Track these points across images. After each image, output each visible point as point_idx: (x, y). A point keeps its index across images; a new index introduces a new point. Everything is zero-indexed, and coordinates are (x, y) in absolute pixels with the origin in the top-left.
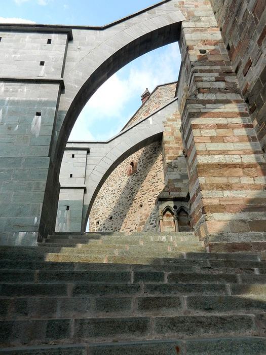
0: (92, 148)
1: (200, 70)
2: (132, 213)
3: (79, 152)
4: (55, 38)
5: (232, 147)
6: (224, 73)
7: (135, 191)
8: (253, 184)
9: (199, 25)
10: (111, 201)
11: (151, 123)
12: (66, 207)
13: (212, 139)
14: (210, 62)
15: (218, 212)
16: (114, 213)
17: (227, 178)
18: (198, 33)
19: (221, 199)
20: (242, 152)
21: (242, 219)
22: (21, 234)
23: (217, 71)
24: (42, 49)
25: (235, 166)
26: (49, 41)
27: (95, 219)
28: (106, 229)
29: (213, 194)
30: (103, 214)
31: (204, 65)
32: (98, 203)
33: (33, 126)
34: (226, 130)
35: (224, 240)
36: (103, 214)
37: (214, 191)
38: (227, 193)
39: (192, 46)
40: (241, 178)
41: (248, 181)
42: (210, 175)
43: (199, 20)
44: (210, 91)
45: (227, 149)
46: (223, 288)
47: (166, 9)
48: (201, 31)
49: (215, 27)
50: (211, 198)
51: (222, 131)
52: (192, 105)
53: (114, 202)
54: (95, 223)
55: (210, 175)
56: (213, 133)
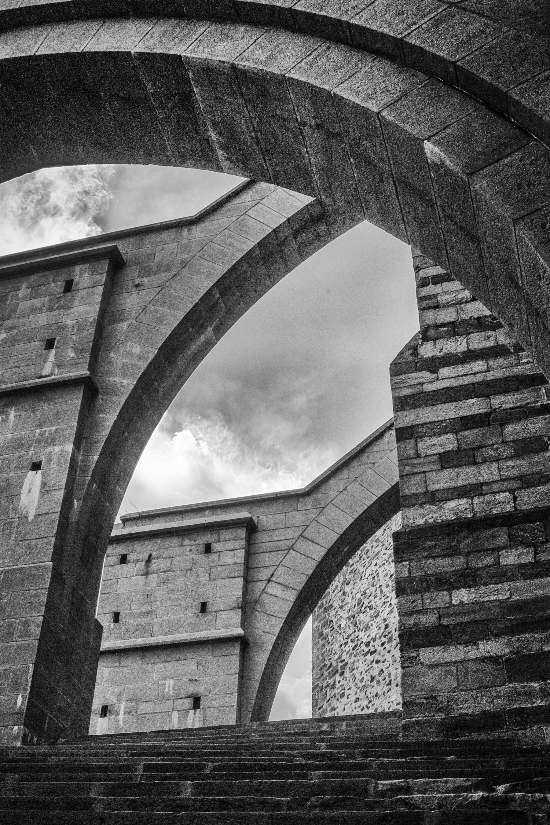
0: (265, 518)
1: (434, 277)
3: (226, 534)
5: (495, 472)
8: (530, 563)
10: (367, 678)
12: (191, 700)
13: (446, 460)
15: (431, 644)
17: (466, 557)
19: (442, 612)
21: (492, 654)
25: (489, 522)
32: (336, 691)
33: (23, 497)
34: (483, 430)
35: (438, 711)
37: (427, 595)
38: (462, 596)
41: (519, 556)
44: (455, 329)
45: (481, 479)
50: (418, 612)
51: (471, 435)
52: (403, 377)
53: (373, 678)
56: (448, 442)
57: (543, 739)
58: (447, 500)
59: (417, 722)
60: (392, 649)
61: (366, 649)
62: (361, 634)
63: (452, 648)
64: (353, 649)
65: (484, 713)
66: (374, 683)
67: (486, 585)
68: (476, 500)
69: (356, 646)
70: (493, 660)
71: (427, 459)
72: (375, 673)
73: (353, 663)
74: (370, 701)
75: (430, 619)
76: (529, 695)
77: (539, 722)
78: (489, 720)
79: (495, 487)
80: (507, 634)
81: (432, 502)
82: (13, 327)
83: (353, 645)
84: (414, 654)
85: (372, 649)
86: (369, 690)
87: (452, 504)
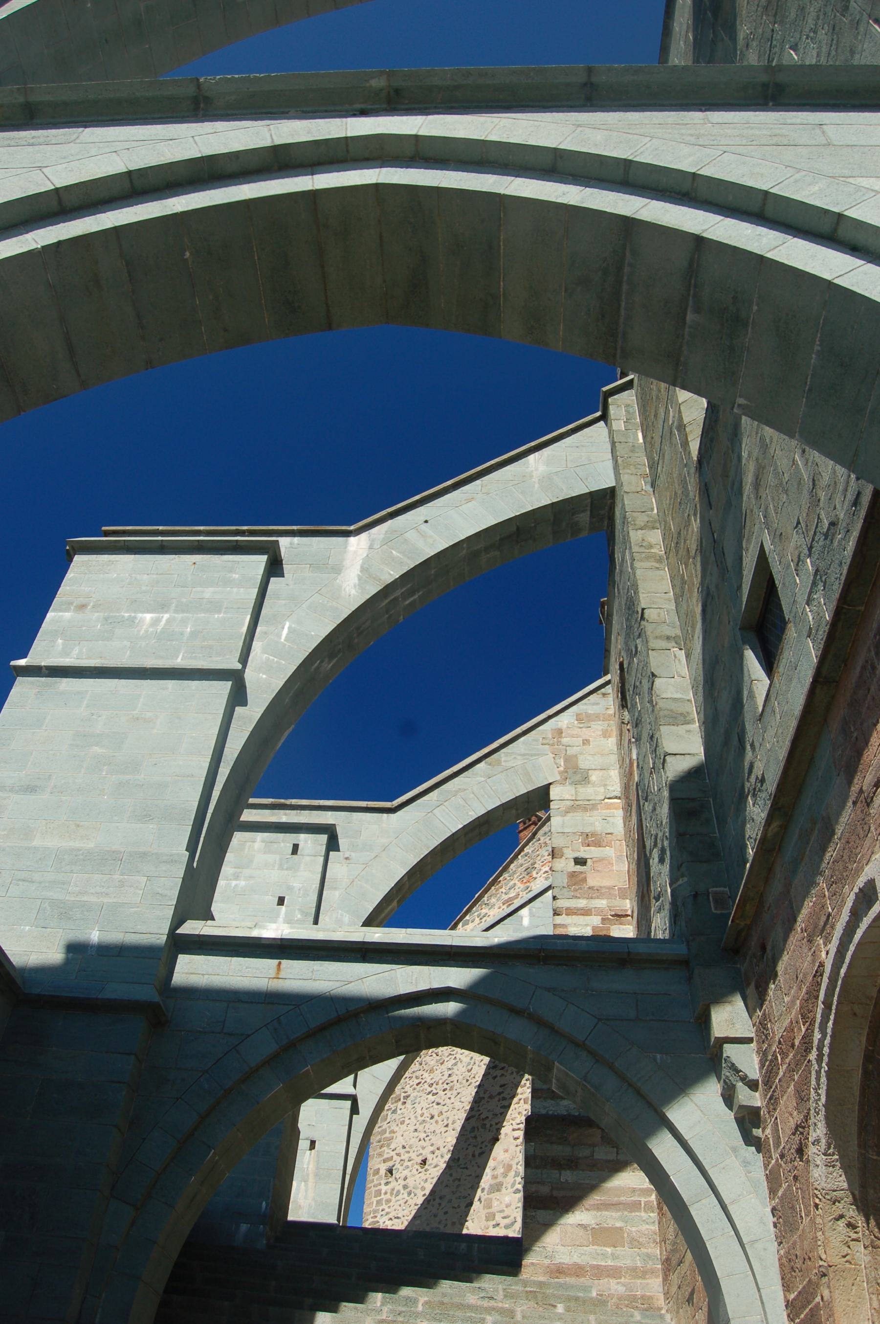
2: (473, 1156)
4: (306, 842)
6: (612, 916)
8: (613, 1161)
9: (587, 792)
11: (526, 922)
12: (309, 1142)
14: (589, 888)
16: (432, 1149)
18: (578, 816)
21: (583, 1222)
22: (244, 1227)
23: (599, 911)
24: (283, 869)
26: (295, 849)
27: (385, 1161)
30: (404, 1147)
31: (576, 897)
32: (395, 1116)
36: (404, 1147)
40: (596, 1149)
43: (585, 779)
47: (523, 751)
48: (585, 809)
49: (616, 798)
50: (538, 1183)
53: (432, 1117)
54: (383, 1172)
57: (610, 1289)
59: (533, 1264)
60: (453, 1097)
61: (429, 1089)
62: (426, 1075)
64: (417, 1085)
66: (433, 1121)
67: (583, 1170)
69: (419, 1083)
70: (584, 1227)
72: (436, 1113)
73: (416, 1098)
74: (427, 1136)
75: (545, 1190)
76: (604, 1256)
77: (608, 1276)
78: (578, 1270)
80: (595, 1209)
82: (251, 877)
83: (418, 1081)
85: (435, 1091)
86: (427, 1126)
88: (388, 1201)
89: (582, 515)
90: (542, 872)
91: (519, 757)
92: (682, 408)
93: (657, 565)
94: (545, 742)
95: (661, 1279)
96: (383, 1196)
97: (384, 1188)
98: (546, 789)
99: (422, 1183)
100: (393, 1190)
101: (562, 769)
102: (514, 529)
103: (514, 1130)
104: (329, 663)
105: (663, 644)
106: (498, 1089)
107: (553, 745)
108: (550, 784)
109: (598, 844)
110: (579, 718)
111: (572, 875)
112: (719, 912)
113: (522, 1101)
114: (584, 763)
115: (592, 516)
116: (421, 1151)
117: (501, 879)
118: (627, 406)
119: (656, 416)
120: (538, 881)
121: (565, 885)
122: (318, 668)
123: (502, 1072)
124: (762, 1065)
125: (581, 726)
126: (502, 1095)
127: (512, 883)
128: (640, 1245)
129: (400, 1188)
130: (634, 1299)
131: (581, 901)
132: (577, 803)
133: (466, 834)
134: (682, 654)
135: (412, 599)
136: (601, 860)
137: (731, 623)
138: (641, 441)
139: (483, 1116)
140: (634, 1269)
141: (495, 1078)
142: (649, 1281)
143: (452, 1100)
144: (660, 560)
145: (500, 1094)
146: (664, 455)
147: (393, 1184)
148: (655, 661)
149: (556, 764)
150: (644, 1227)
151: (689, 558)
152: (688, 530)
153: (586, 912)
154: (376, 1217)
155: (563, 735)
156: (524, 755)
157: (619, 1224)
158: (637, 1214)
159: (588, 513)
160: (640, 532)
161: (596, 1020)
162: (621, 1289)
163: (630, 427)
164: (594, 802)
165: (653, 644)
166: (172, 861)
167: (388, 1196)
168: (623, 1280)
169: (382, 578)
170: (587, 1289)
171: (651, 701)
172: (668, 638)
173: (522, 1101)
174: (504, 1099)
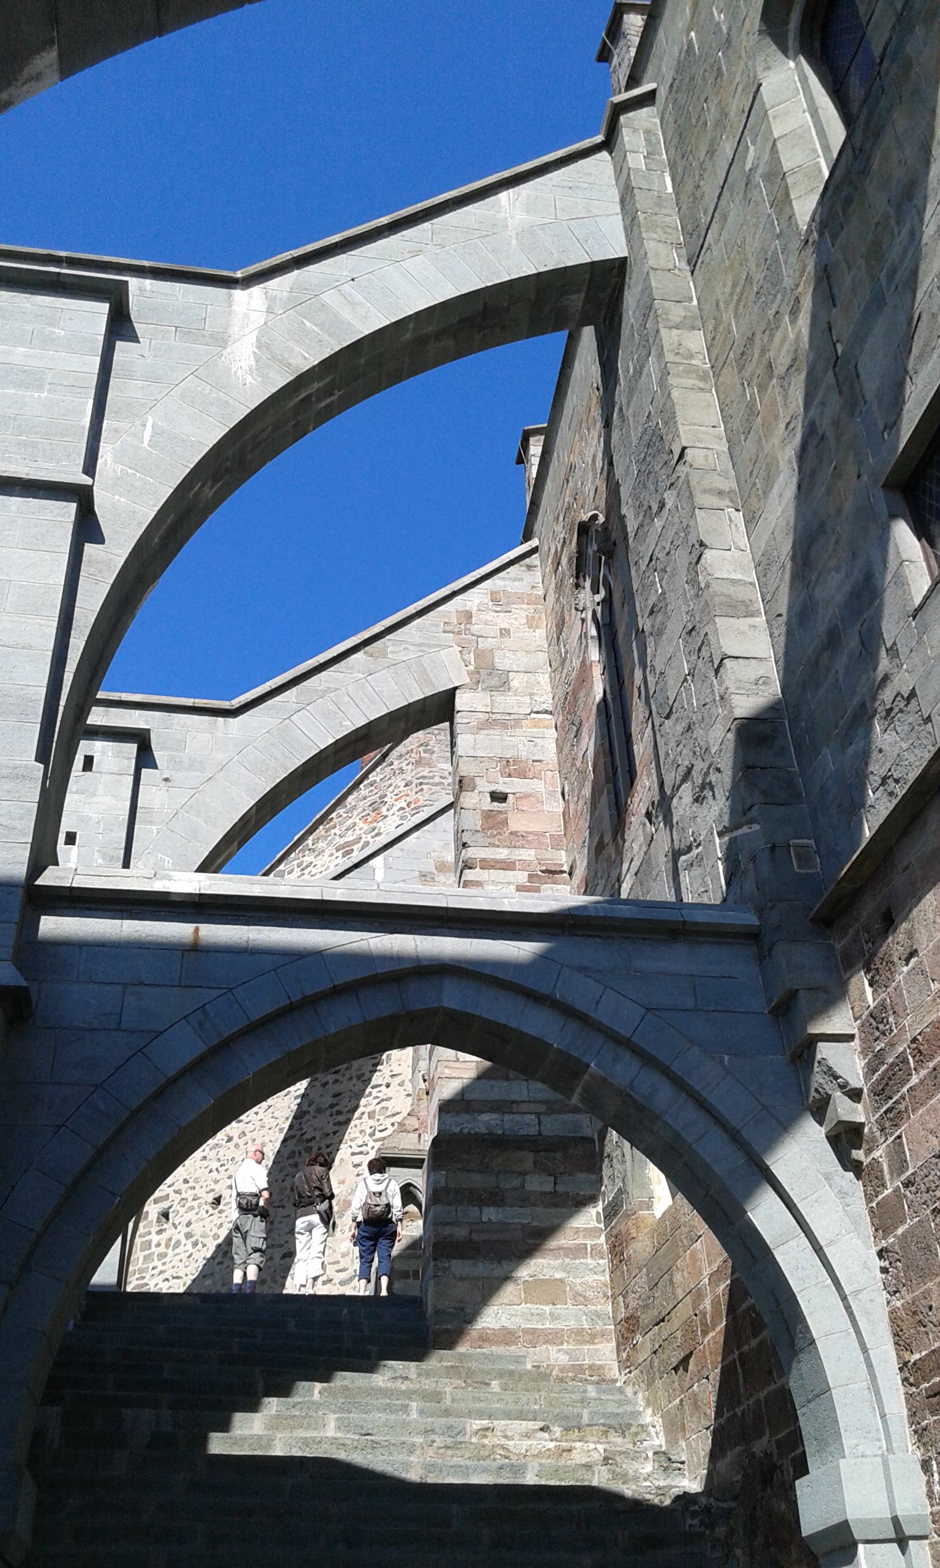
1: (483, 860)
4: (104, 753)
5: (525, 1092)
6: (542, 872)
7: (312, 1109)
8: (550, 1193)
9: (506, 702)
11: (379, 876)
14: (511, 833)
17: (497, 1176)
18: (495, 734)
20: (542, 1108)
23: (525, 865)
28: (195, 1244)
29: (460, 1215)
30: (186, 1181)
31: (494, 845)
36: (186, 1181)
37: (460, 1208)
38: (491, 1214)
39: (473, 779)
40: (528, 1177)
41: (541, 1184)
42: (460, 1166)
43: (504, 685)
45: (513, 1097)
46: (405, 1408)
47: (417, 640)
48: (504, 725)
49: (546, 712)
53: (230, 1139)
55: (460, 1166)
57: (549, 1359)
58: (482, 1112)
63: (480, 1264)
65: (504, 1328)
68: (507, 1117)
71: (465, 1065)
75: (461, 1233)
76: (541, 1316)
77: (546, 1342)
79: (524, 1107)
81: (467, 1112)
84: (447, 1265)
86: (222, 1151)
87: (485, 1117)
88: (163, 1256)
89: (574, 297)
90: (395, 809)
91: (411, 648)
92: (779, 145)
93: (701, 384)
94: (447, 628)
95: (614, 1344)
96: (153, 1249)
97: (155, 1238)
98: (451, 693)
99: (215, 1230)
100: (170, 1239)
101: (472, 668)
102: (481, 307)
103: (353, 1154)
104: (212, 487)
105: (715, 501)
106: (330, 1100)
107: (459, 633)
108: (456, 688)
109: (522, 775)
110: (495, 598)
111: (488, 815)
112: (802, 871)
113: (366, 1116)
114: (503, 661)
115: (587, 300)
116: (213, 1186)
117: (333, 815)
118: (647, 132)
119: (711, 153)
120: (389, 820)
121: (478, 828)
122: (197, 494)
123: (335, 1076)
124: (871, 1069)
125: (499, 609)
126: (337, 1108)
127: (351, 821)
128: (586, 1301)
129: (182, 1237)
130: (580, 1369)
131: (500, 850)
132: (494, 717)
133: (336, 753)
134: (739, 518)
135: (328, 401)
136: (527, 796)
137: (865, 478)
138: (670, 190)
139: (307, 1136)
140: (579, 1332)
141: (325, 1084)
142: (599, 1346)
143: (260, 1116)
144: (704, 378)
145: (332, 1106)
146: (725, 218)
147: (170, 1231)
148: (704, 524)
149: (464, 661)
150: (591, 1279)
151: (771, 378)
152: (772, 336)
153: (507, 866)
154: (143, 1278)
155: (474, 620)
156: (420, 645)
157: (558, 1276)
158: (582, 1261)
159: (583, 294)
160: (675, 332)
161: (644, 1011)
162: (563, 1359)
163: (653, 166)
164: (516, 717)
165: (700, 499)
166: (16, 776)
167: (162, 1249)
168: (565, 1346)
169: (292, 361)
170: (519, 1359)
171: (693, 582)
172: (720, 493)
173: (366, 1116)
174: (339, 1113)
